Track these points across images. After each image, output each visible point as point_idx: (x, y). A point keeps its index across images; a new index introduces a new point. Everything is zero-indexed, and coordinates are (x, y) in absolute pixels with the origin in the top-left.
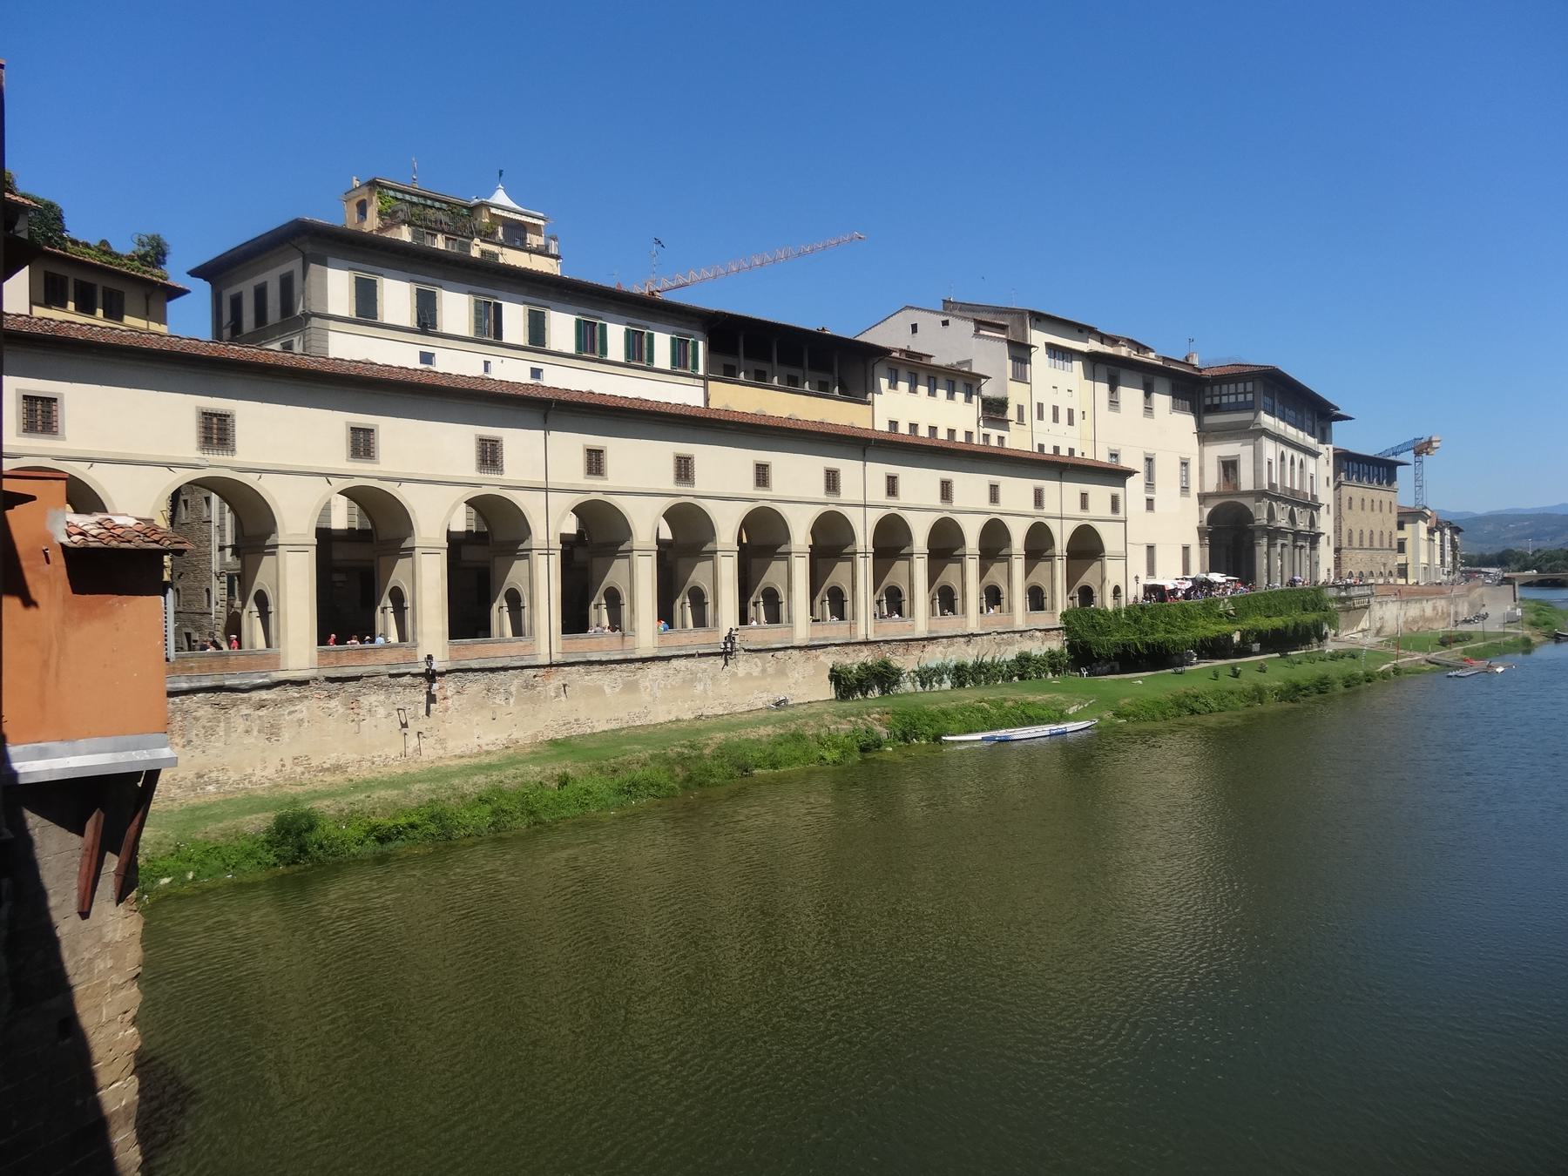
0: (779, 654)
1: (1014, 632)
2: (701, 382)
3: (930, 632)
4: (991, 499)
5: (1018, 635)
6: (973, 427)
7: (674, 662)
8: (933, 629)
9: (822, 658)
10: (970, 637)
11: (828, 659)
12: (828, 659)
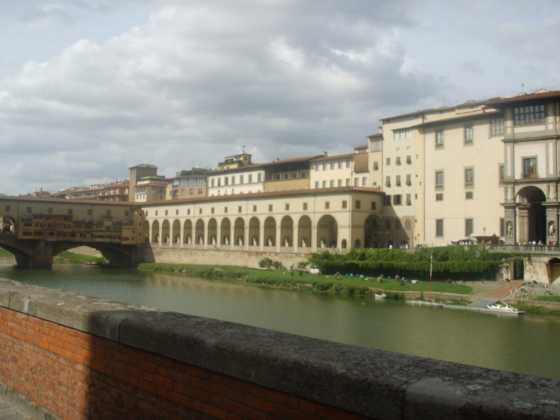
1: (293, 253)
2: (262, 184)
6: (349, 176)
9: (237, 254)
10: (276, 254)
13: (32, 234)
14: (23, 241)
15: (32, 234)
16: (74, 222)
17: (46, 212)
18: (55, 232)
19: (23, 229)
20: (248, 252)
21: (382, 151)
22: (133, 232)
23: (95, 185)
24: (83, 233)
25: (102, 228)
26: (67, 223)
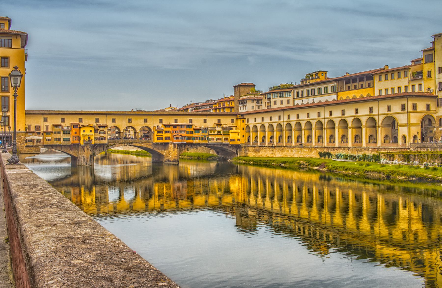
0: (311, 148)
3: (339, 146)
4: (413, 108)
5: (363, 149)
6: (407, 84)
7: (297, 148)
8: (340, 146)
9: (317, 150)
10: (349, 149)
11: (319, 150)
12: (319, 150)
13: (164, 139)
14: (157, 144)
15: (164, 139)
16: (194, 129)
17: (173, 123)
19: (157, 135)
20: (326, 147)
21: (435, 62)
22: (238, 134)
23: (209, 101)
24: (201, 137)
25: (214, 133)
26: (189, 130)
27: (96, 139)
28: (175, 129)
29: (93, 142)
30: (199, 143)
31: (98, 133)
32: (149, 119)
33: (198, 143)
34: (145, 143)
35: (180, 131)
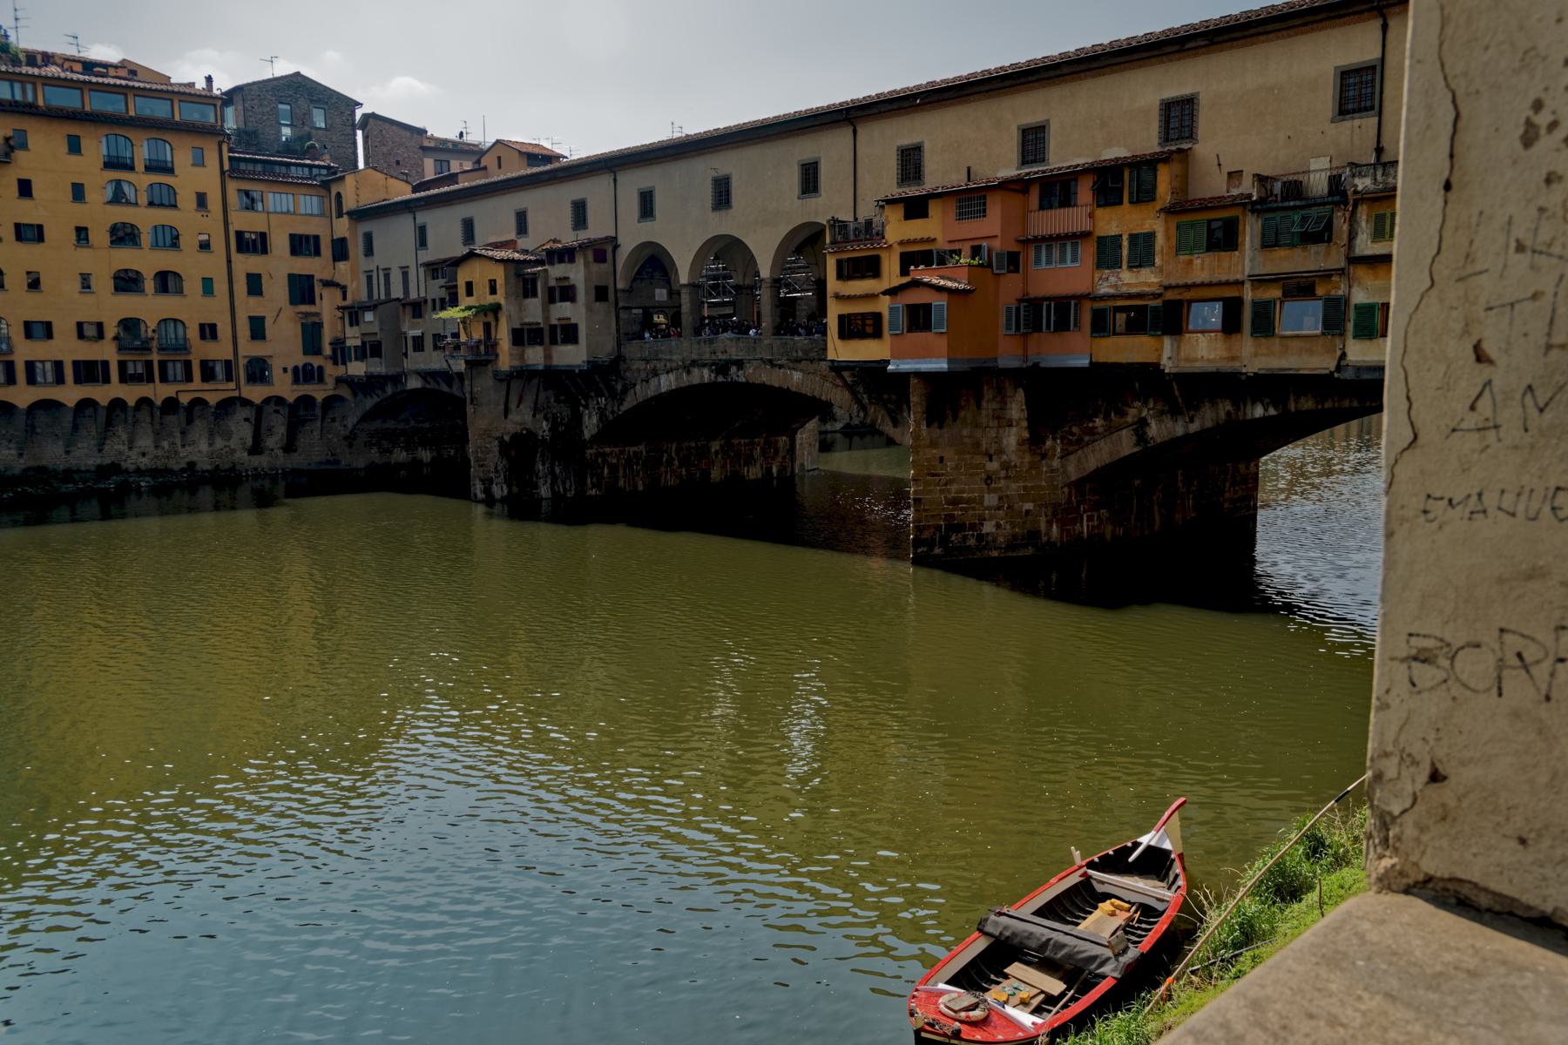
18: (939, 301)
19: (837, 297)
24: (1248, 295)
26: (1117, 222)
27: (521, 337)
28: (974, 228)
29: (506, 358)
30: (1227, 366)
31: (535, 295)
32: (831, 150)
33: (1211, 368)
34: (812, 367)
35: (1038, 241)
